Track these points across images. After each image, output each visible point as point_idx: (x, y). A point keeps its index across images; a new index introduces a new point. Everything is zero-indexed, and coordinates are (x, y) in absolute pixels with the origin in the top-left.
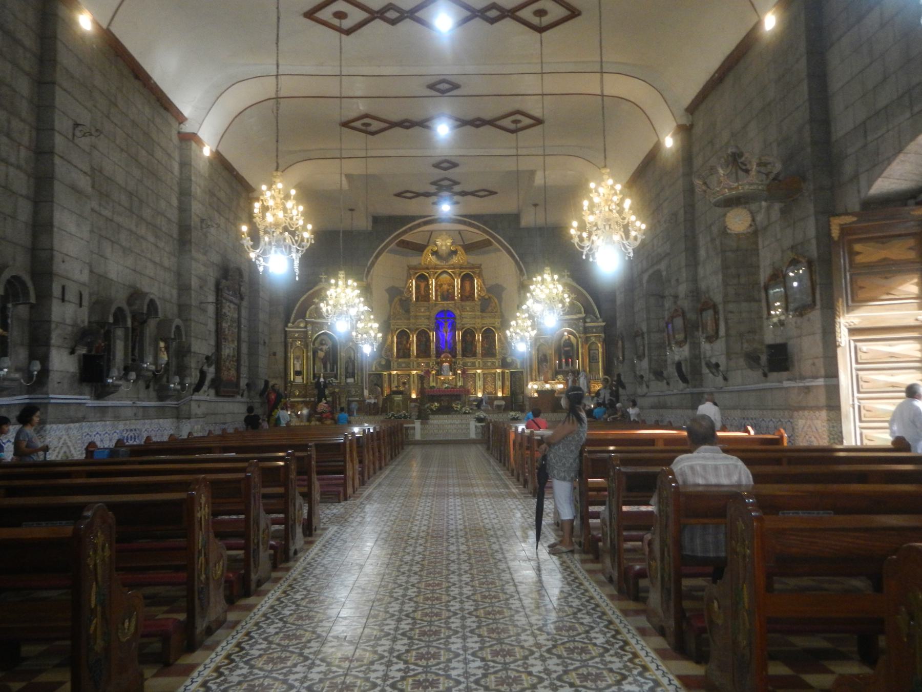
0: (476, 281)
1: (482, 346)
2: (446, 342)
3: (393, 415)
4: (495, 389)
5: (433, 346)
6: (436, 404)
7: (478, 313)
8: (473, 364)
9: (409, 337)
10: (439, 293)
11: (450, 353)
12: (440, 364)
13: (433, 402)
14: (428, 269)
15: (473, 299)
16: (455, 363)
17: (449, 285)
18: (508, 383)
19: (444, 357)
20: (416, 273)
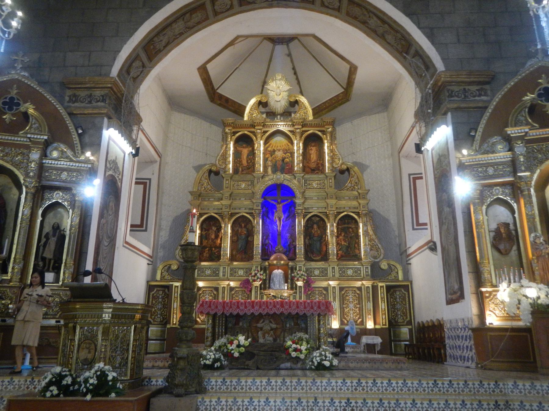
0: (326, 145)
1: (338, 244)
2: (281, 234)
3: (58, 380)
4: (361, 315)
5: (258, 240)
6: (241, 338)
7: (332, 191)
8: (324, 274)
9: (219, 228)
10: (269, 163)
11: (284, 253)
12: (268, 270)
13: (235, 334)
14: (253, 126)
15: (323, 171)
16: (293, 269)
17: (286, 151)
18: (383, 306)
19: (275, 259)
20: (235, 133)
